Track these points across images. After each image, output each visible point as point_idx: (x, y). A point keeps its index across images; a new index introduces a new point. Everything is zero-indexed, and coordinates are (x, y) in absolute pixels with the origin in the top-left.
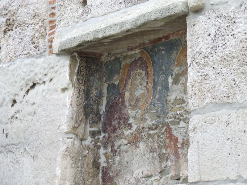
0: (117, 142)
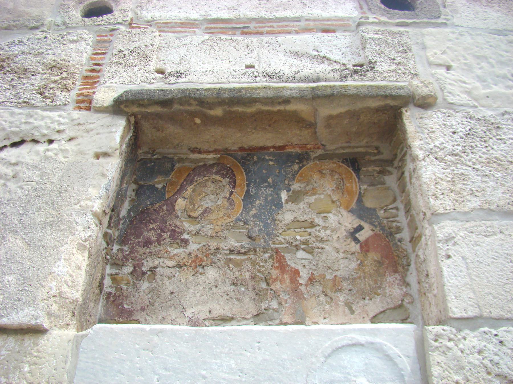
0: (147, 261)
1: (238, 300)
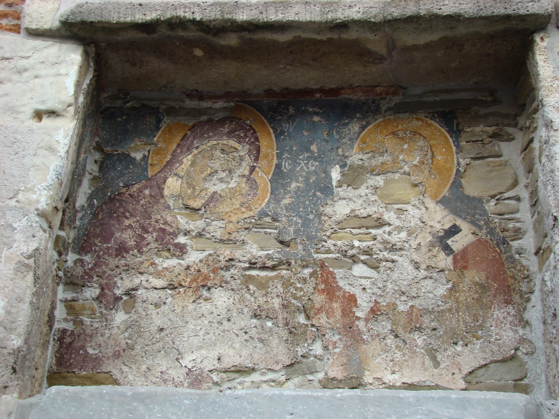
0: (122, 279)
1: (261, 341)
